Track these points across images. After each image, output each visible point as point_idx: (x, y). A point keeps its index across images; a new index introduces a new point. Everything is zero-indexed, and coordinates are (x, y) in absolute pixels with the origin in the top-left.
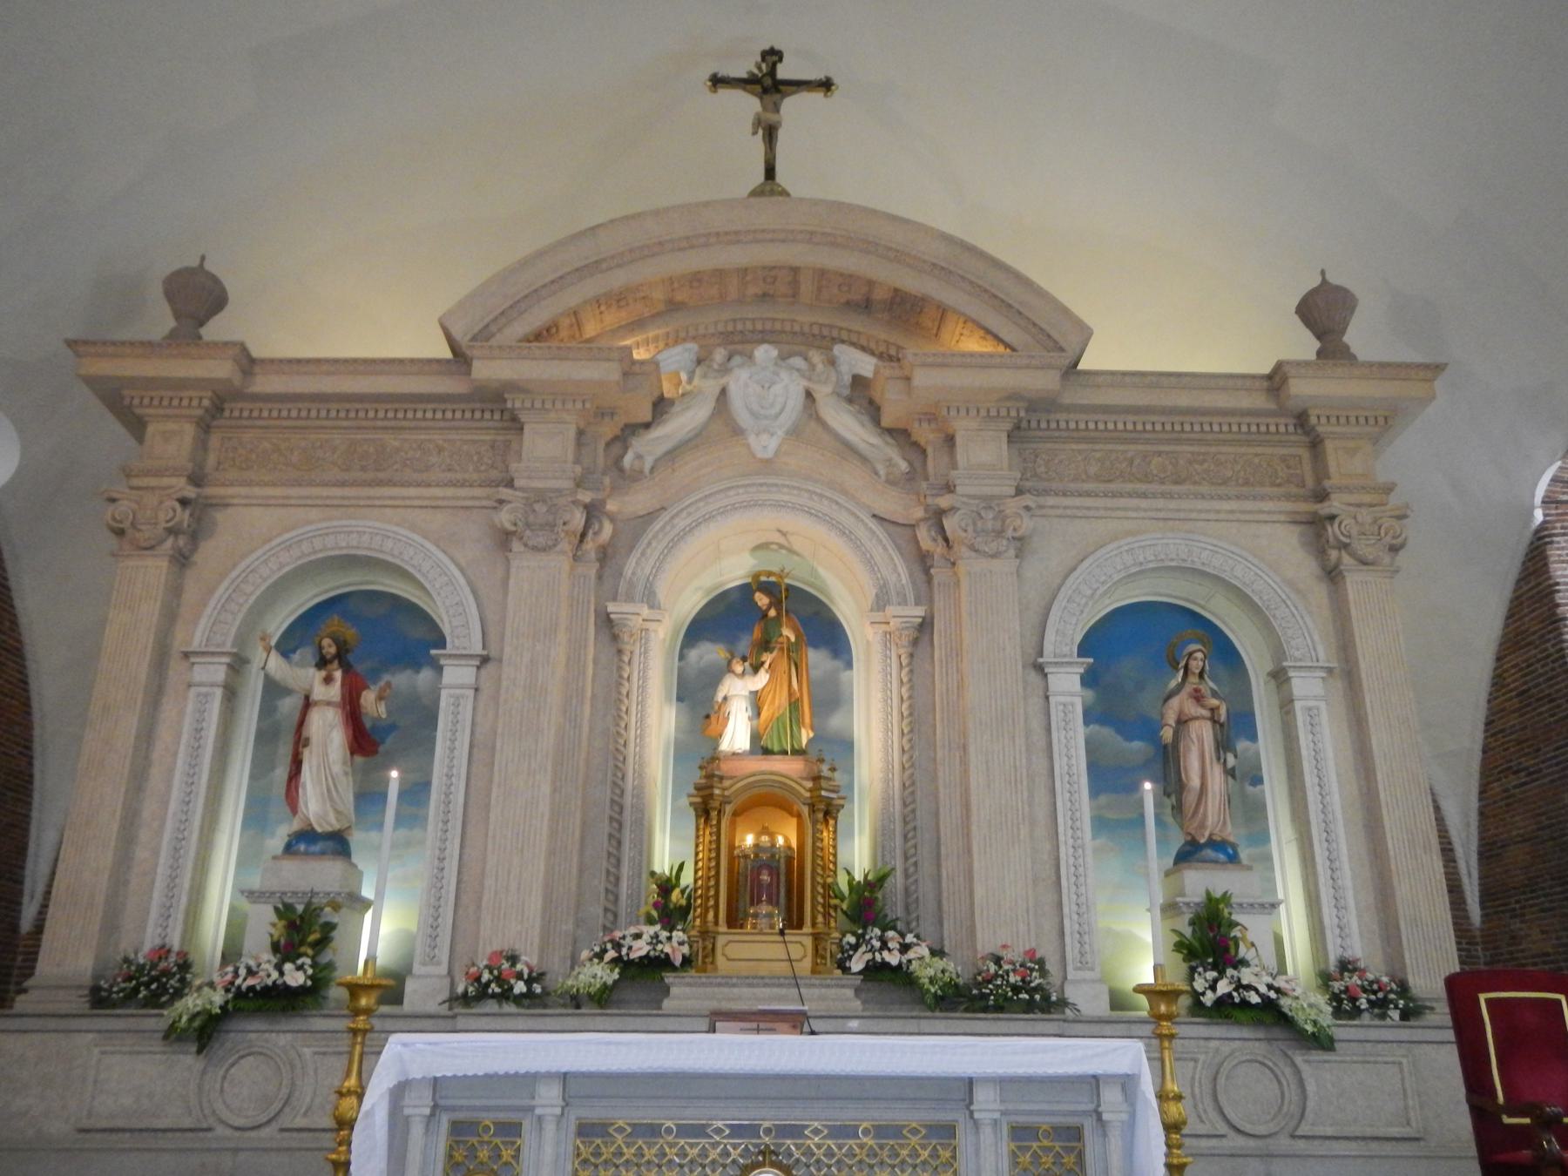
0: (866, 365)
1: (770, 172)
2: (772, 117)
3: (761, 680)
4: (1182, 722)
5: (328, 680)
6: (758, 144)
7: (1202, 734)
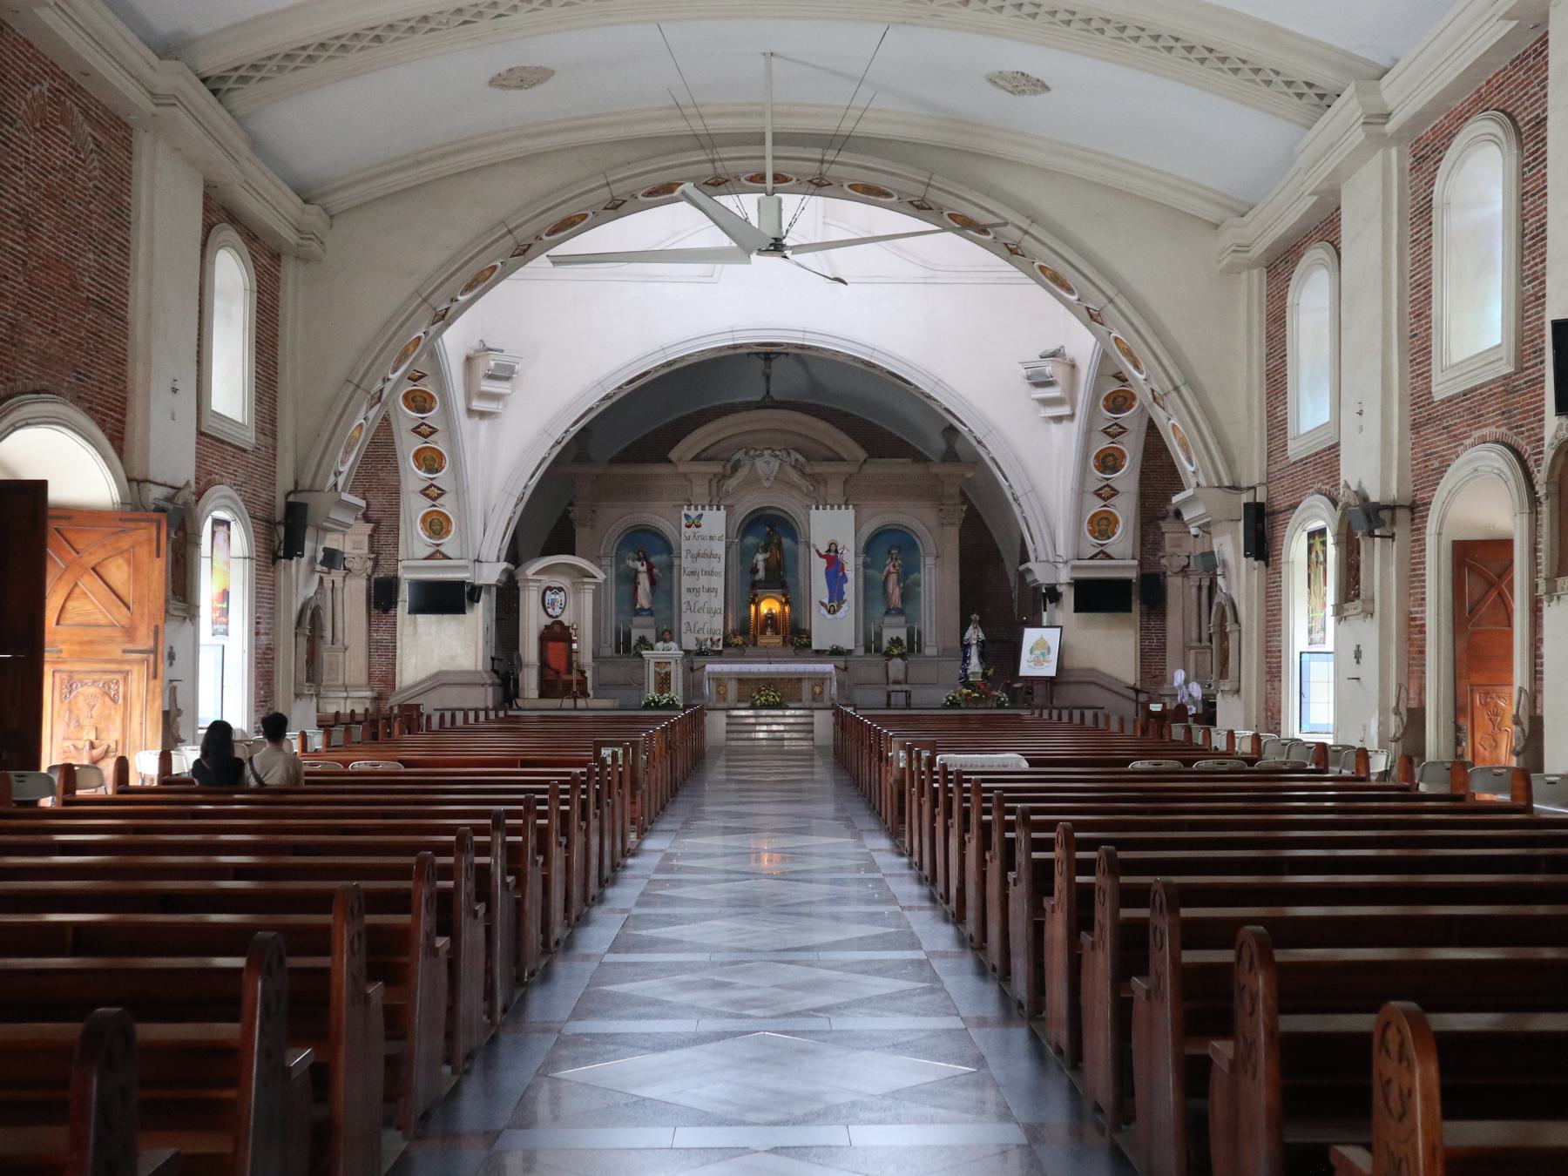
0: (802, 459)
1: (768, 392)
2: (769, 371)
3: (767, 555)
4: (889, 573)
5: (642, 565)
6: (764, 380)
7: (893, 578)
